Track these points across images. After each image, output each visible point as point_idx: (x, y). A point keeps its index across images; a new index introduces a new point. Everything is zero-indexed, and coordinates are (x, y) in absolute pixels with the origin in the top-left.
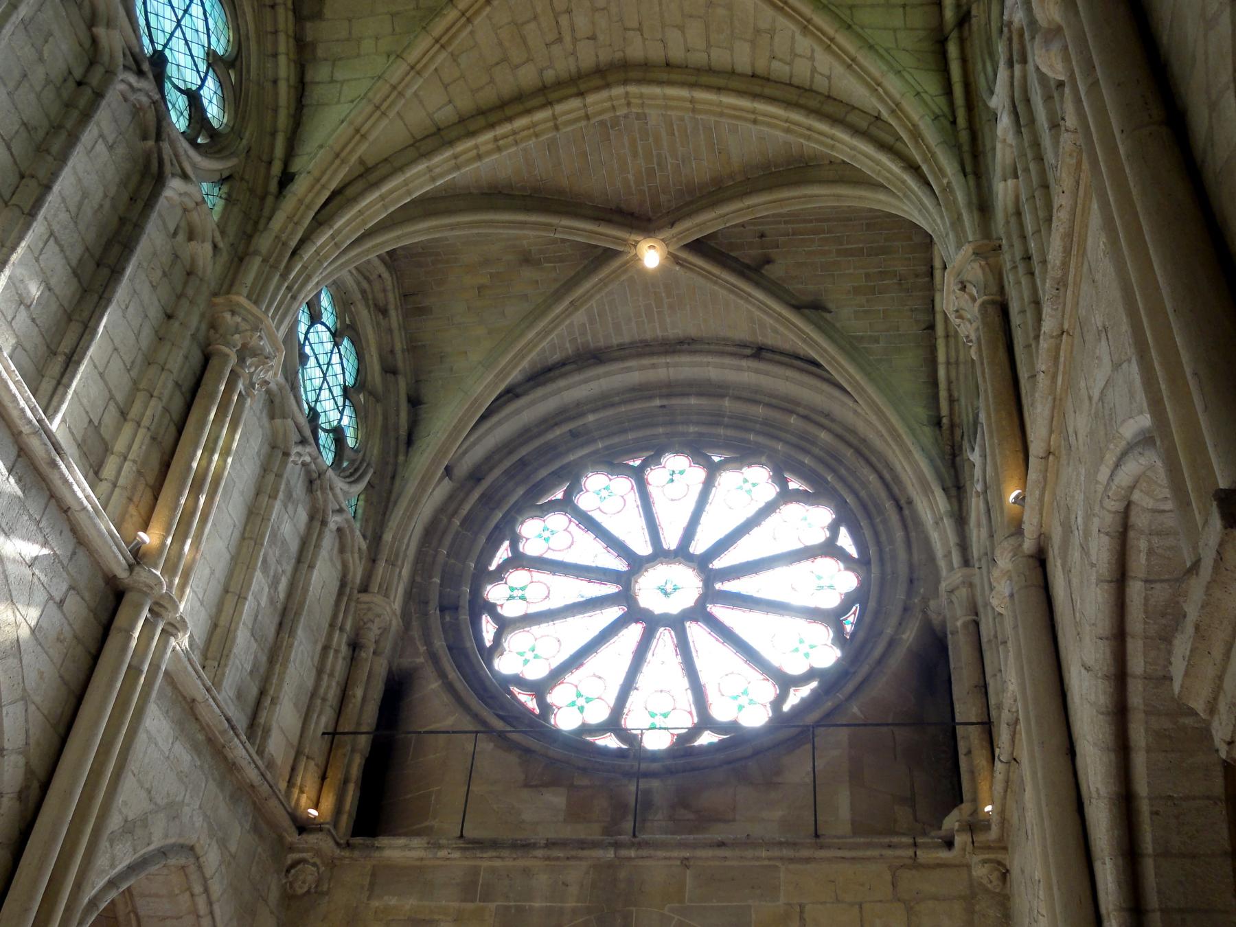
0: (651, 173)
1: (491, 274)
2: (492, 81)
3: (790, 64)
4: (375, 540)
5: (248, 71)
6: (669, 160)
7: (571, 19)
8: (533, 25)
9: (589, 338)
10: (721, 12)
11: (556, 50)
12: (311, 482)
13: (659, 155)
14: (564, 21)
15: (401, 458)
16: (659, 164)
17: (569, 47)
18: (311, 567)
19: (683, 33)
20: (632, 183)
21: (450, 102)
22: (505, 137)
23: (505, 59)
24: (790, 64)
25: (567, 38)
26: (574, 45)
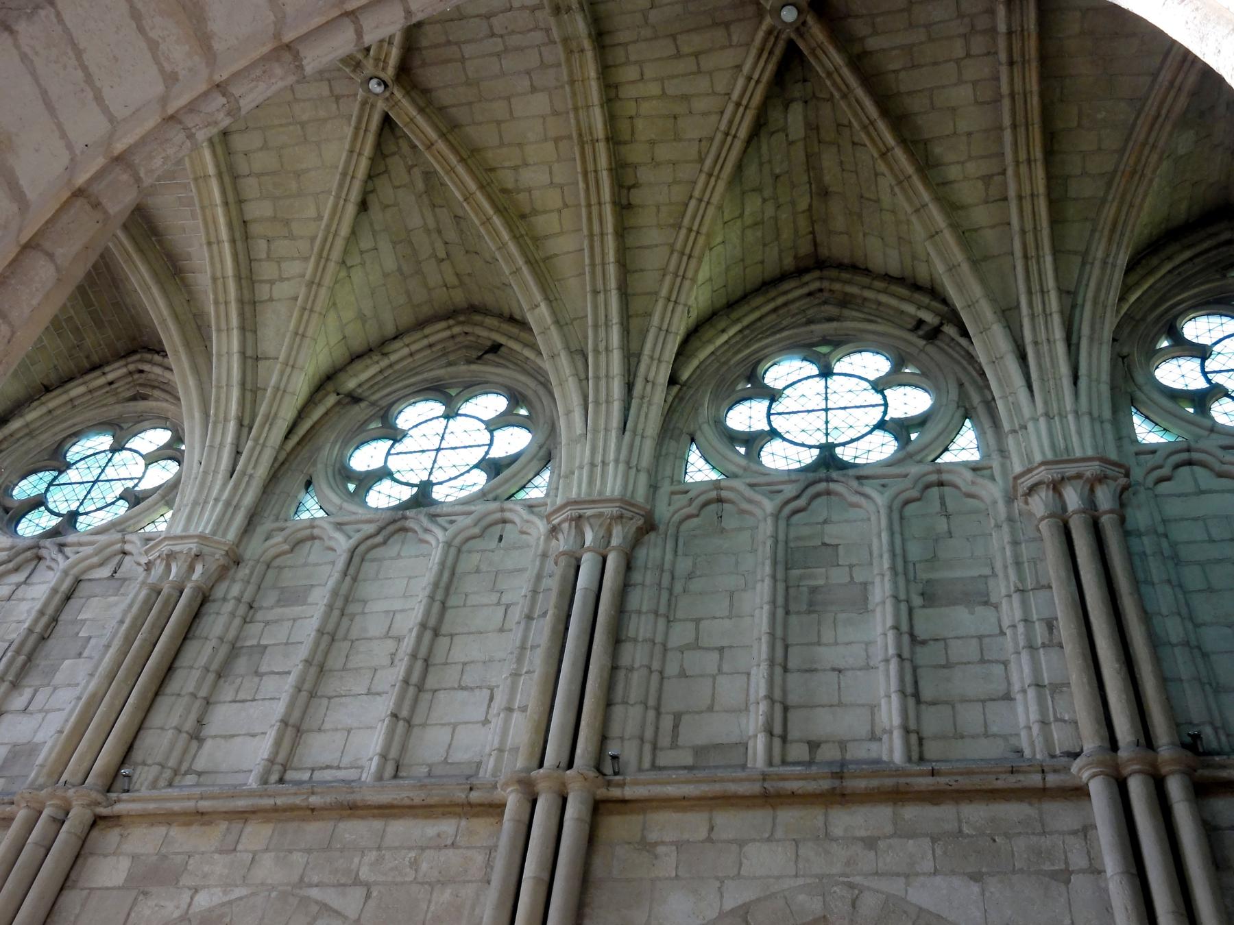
3: (269, 258)
10: (294, 185)
19: (261, 149)
24: (269, 258)
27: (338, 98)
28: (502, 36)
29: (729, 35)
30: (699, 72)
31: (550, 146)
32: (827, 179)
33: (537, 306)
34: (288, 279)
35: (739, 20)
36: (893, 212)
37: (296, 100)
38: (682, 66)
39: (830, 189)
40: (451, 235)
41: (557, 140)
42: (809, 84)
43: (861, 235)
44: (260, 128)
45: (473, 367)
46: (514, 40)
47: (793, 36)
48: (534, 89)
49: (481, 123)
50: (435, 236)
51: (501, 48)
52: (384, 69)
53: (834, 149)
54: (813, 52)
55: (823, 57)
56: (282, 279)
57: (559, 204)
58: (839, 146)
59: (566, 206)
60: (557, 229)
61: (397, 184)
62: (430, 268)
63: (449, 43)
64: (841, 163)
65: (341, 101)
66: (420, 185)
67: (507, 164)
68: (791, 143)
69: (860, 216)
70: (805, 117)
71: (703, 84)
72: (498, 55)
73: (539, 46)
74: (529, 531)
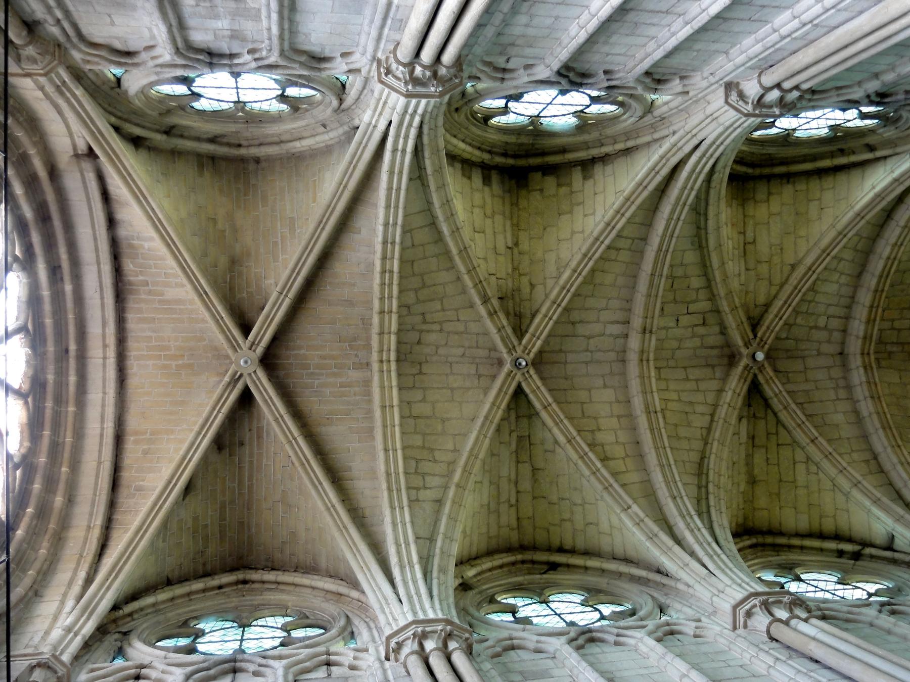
0: (307, 367)
1: (224, 231)
2: (414, 275)
3: (416, 472)
4: (79, 76)
5: (475, 125)
6: (317, 382)
7: (436, 331)
8: (439, 307)
9: (143, 296)
10: (440, 428)
11: (419, 319)
12: (210, 54)
13: (323, 374)
14: (436, 327)
15: (113, 120)
16: (312, 373)
17: (417, 327)
18: (170, 27)
19: (421, 401)
20: (296, 352)
21: (413, 245)
22: (391, 278)
23: (424, 286)
25: (424, 327)
26: (418, 331)
27: (480, 376)
28: (591, 352)
29: (714, 373)
30: (698, 390)
31: (615, 420)
32: (756, 471)
33: (629, 507)
34: (430, 488)
35: (719, 365)
36: (807, 487)
37: (452, 373)
38: (691, 385)
39: (757, 479)
40: (526, 485)
41: (619, 417)
42: (752, 408)
43: (778, 508)
44: (421, 388)
45: (545, 576)
46: (598, 356)
47: (757, 372)
48: (605, 386)
49: (570, 403)
50: (512, 485)
51: (589, 359)
52: (528, 354)
53: (763, 450)
54: (767, 381)
55: (773, 385)
56: (425, 488)
57: (623, 455)
58: (767, 449)
59: (627, 456)
60: (624, 469)
61: (502, 441)
62: (504, 508)
63: (561, 351)
64: (768, 459)
65: (481, 379)
66: (514, 446)
67: (586, 429)
68: (740, 444)
69: (778, 495)
70: (748, 429)
71: (700, 397)
72: (586, 363)
73: (610, 362)
74: (702, 634)
